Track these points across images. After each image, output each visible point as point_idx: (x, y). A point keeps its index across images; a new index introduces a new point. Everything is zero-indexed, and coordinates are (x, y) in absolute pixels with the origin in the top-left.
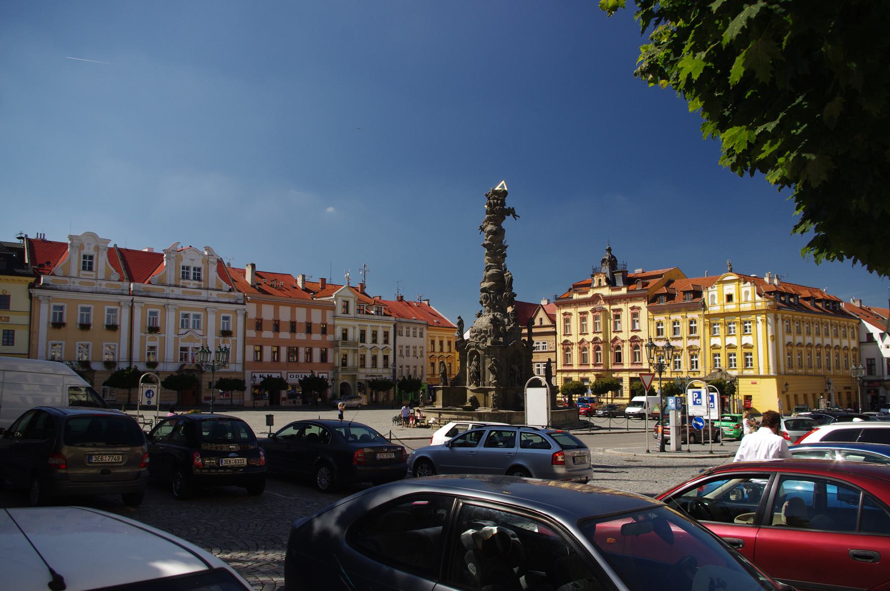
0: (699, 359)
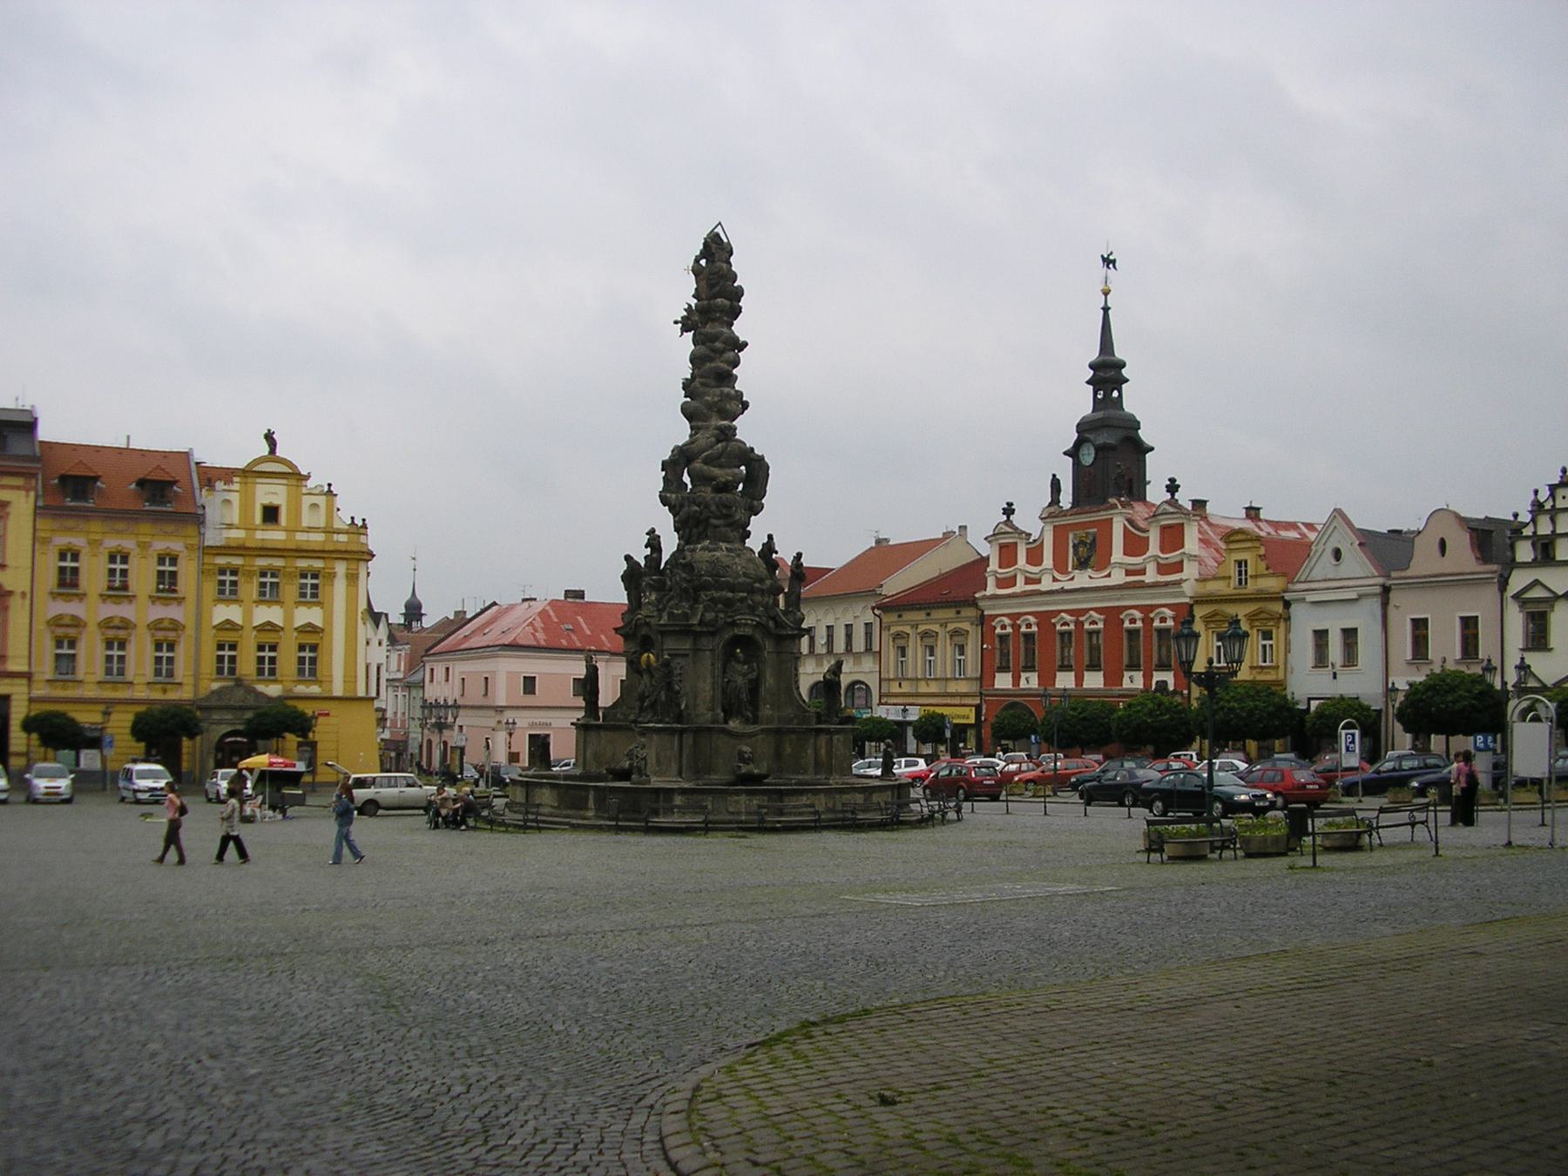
0: (182, 655)
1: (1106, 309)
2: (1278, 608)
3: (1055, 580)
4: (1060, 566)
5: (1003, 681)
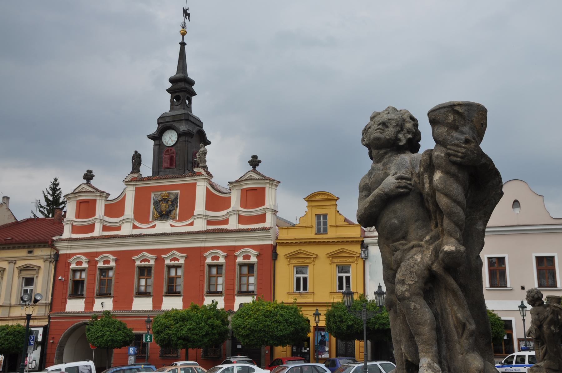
1: (183, 44)
2: (357, 249)
3: (135, 227)
4: (141, 215)
5: (75, 306)
